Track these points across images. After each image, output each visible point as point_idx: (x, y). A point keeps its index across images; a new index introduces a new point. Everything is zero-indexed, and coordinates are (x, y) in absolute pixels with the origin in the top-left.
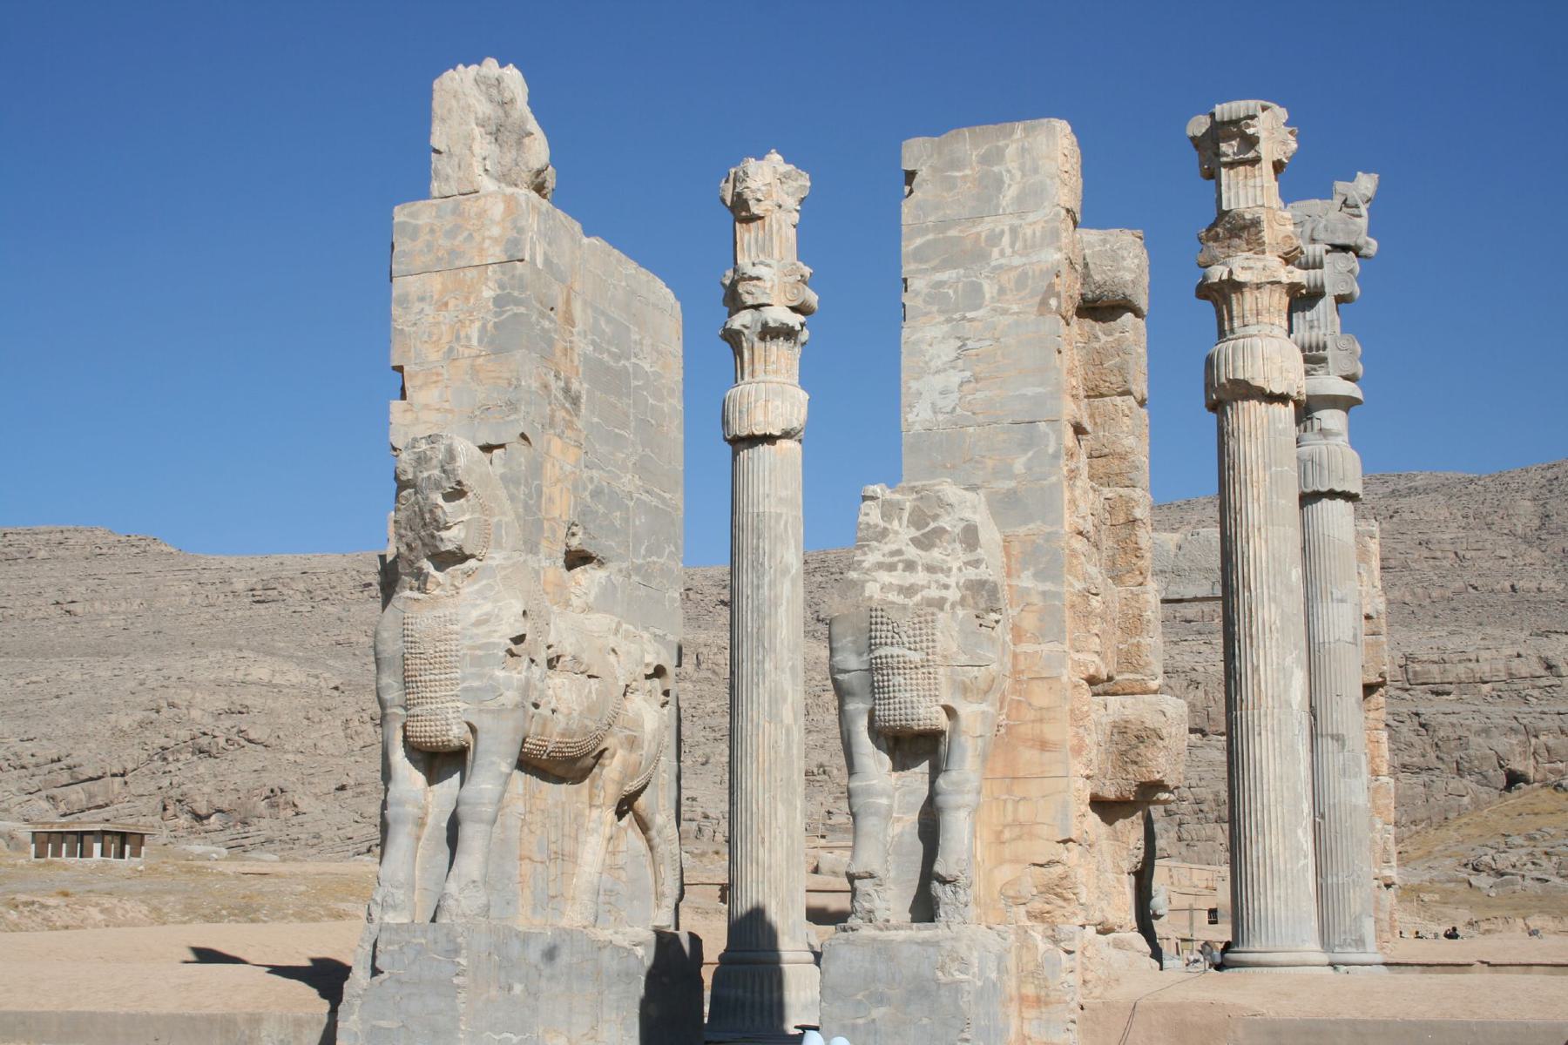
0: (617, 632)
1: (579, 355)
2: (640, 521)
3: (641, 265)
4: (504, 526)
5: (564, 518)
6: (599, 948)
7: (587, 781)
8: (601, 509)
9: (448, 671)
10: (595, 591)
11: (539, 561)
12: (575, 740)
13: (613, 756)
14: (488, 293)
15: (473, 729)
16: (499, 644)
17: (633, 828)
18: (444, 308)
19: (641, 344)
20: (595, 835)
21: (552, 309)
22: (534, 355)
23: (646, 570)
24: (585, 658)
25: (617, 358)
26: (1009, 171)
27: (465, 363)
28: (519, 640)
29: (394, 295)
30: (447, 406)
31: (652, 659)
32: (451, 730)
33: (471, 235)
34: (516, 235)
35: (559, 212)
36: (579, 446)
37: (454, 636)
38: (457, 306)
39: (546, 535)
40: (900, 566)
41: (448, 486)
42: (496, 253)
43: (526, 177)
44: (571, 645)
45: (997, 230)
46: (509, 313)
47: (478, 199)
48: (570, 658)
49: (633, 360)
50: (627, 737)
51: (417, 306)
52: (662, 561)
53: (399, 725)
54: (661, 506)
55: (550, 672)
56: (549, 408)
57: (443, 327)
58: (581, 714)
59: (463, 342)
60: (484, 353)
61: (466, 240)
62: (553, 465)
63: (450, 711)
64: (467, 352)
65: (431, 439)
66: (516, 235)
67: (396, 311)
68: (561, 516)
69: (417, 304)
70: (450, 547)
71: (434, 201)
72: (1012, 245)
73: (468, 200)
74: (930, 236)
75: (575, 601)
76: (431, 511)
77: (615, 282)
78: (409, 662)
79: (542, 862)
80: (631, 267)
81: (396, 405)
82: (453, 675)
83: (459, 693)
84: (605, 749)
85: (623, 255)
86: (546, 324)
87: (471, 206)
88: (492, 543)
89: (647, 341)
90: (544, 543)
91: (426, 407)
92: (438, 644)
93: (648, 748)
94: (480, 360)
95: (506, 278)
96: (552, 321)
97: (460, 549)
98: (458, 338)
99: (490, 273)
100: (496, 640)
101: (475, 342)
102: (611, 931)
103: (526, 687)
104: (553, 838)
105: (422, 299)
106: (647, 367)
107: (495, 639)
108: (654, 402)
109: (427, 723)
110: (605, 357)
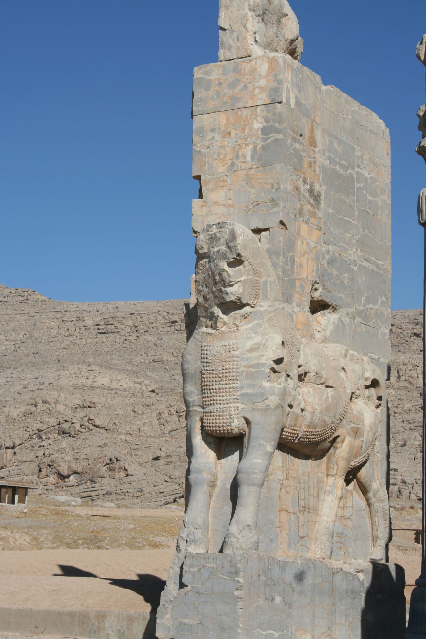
0: (345, 356)
1: (319, 167)
2: (361, 280)
3: (362, 104)
4: (269, 284)
5: (309, 278)
6: (334, 574)
7: (325, 458)
8: (335, 272)
10: (331, 328)
11: (293, 307)
12: (317, 430)
13: (343, 441)
14: (258, 125)
15: (248, 422)
16: (266, 364)
17: (356, 491)
18: (228, 136)
19: (362, 158)
20: (331, 495)
21: (301, 135)
22: (289, 167)
23: (366, 314)
24: (324, 374)
25: (346, 168)
27: (241, 173)
28: (279, 361)
29: (194, 127)
30: (230, 202)
31: (370, 375)
32: (233, 422)
33: (246, 86)
34: (277, 85)
35: (306, 68)
36: (320, 229)
37: (235, 359)
38: (236, 134)
39: (297, 290)
41: (231, 257)
42: (263, 98)
43: (284, 45)
44: (314, 365)
46: (272, 139)
47: (251, 61)
48: (314, 374)
49: (357, 169)
50: (353, 429)
51: (210, 135)
52: (377, 307)
53: (198, 418)
54: (376, 270)
55: (300, 384)
56: (299, 203)
57: (227, 149)
58: (321, 412)
59: (241, 159)
60: (255, 166)
61: (242, 89)
62: (302, 242)
64: (244, 166)
65: (220, 225)
66: (277, 85)
67: (196, 138)
68: (307, 277)
69: (209, 133)
70: (233, 298)
71: (221, 63)
73: (244, 62)
75: (317, 335)
76: (220, 274)
77: (345, 116)
78: (205, 376)
79: (294, 513)
80: (355, 105)
81: (196, 203)
82: (234, 385)
83: (239, 397)
84: (338, 437)
85: (350, 98)
86: (297, 146)
87: (246, 66)
88: (261, 296)
89: (366, 157)
90: (296, 296)
91: (216, 203)
92: (224, 364)
93: (367, 436)
94: (253, 170)
95: (270, 115)
96: (301, 144)
97: (239, 299)
98: (237, 157)
99: (259, 112)
100: (264, 362)
101: (249, 159)
102: (342, 562)
103: (284, 393)
104: (302, 497)
105: (213, 130)
106: (366, 175)
107: (263, 360)
108: (371, 198)
109: (217, 418)
110: (338, 168)
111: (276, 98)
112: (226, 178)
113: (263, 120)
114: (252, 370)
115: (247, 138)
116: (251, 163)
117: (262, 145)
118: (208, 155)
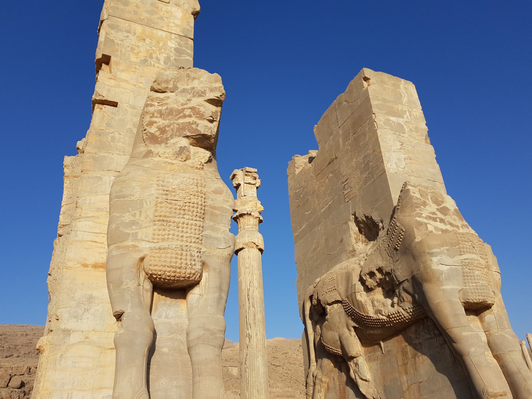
9: (198, 219)
18: (142, 41)
26: (403, 92)
30: (141, 85)
32: (195, 265)
40: (438, 220)
45: (404, 109)
51: (126, 34)
63: (196, 251)
64: (156, 65)
72: (411, 116)
74: (381, 102)
91: (127, 81)
98: (151, 57)
100: (228, 207)
101: (162, 62)
111: (189, 35)
112: (138, 67)
113: (177, 44)
114: (217, 212)
115: (162, 49)
116: (165, 66)
117: (175, 58)
118: (122, 46)
